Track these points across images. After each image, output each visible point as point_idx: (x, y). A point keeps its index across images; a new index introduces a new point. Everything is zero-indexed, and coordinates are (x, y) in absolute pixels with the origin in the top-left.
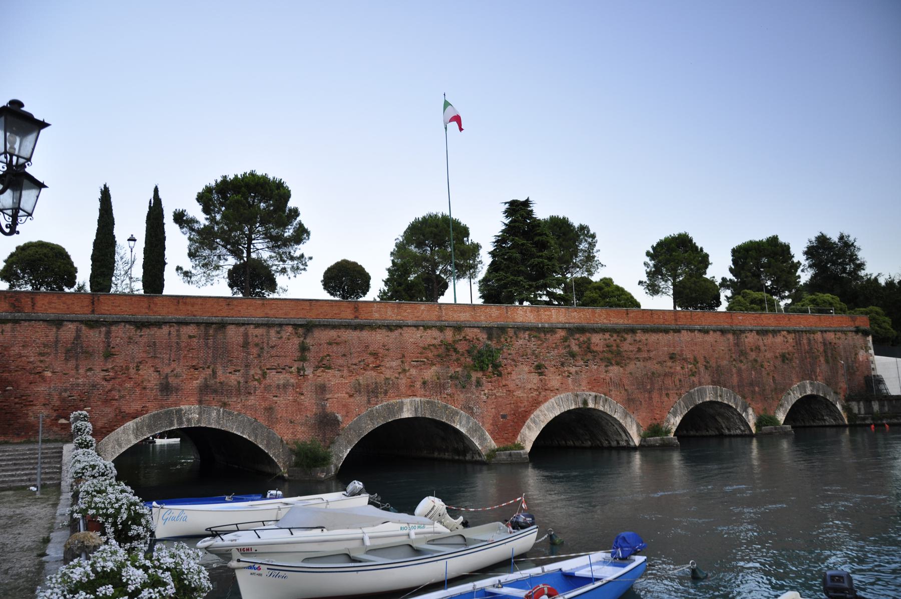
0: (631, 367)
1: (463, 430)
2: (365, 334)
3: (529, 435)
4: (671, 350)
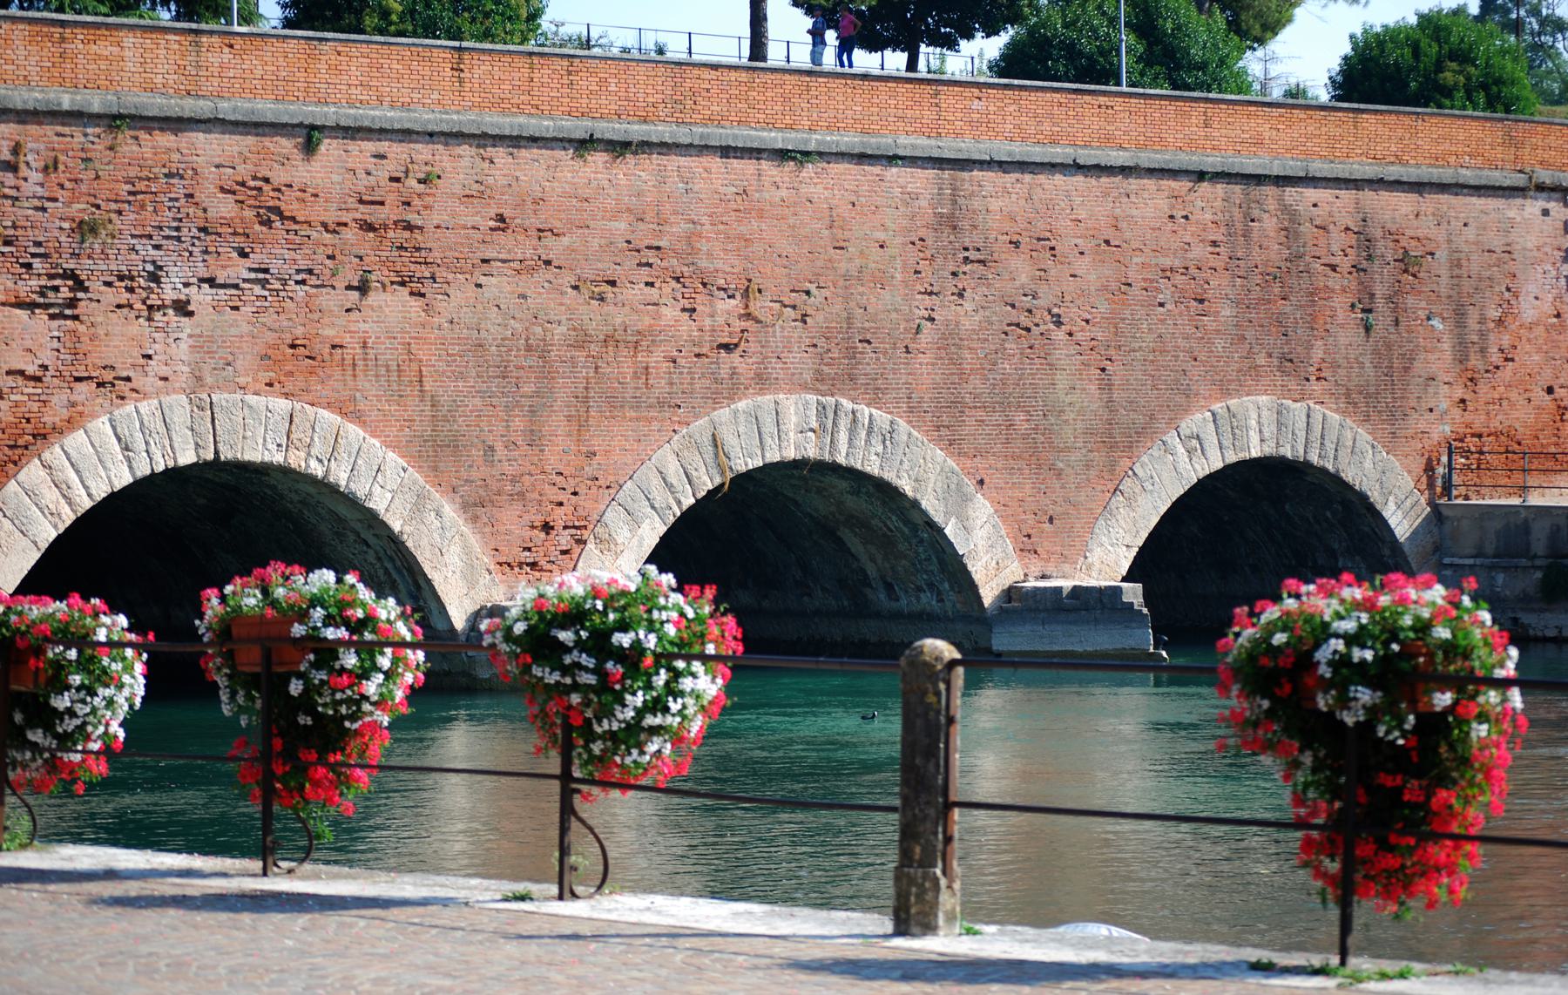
0: (458, 299)
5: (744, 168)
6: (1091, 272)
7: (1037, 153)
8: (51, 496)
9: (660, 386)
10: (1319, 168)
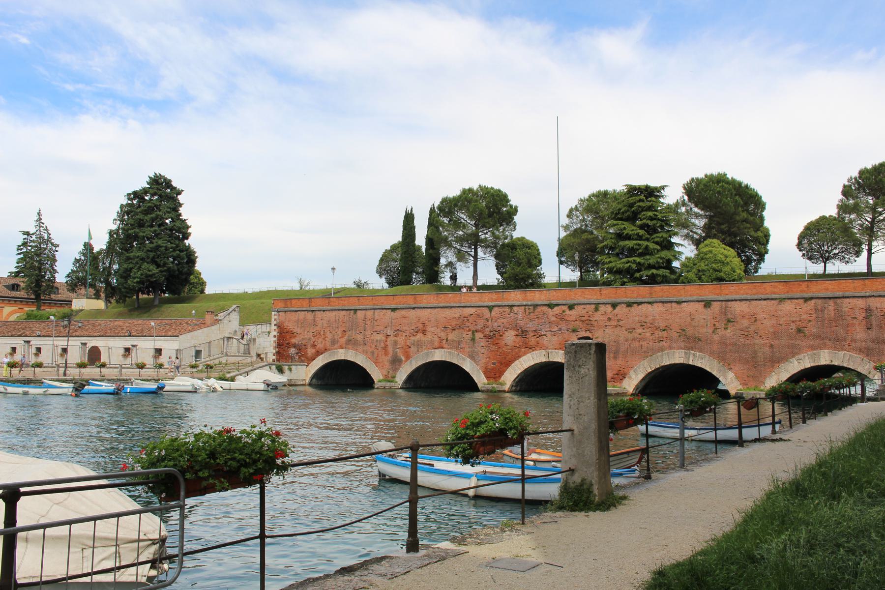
1: (467, 370)
2: (418, 312)
3: (510, 376)
4: (643, 319)
5: (669, 305)
6: (768, 323)
7: (749, 297)
8: (520, 366)
9: (645, 349)
10: (847, 294)
